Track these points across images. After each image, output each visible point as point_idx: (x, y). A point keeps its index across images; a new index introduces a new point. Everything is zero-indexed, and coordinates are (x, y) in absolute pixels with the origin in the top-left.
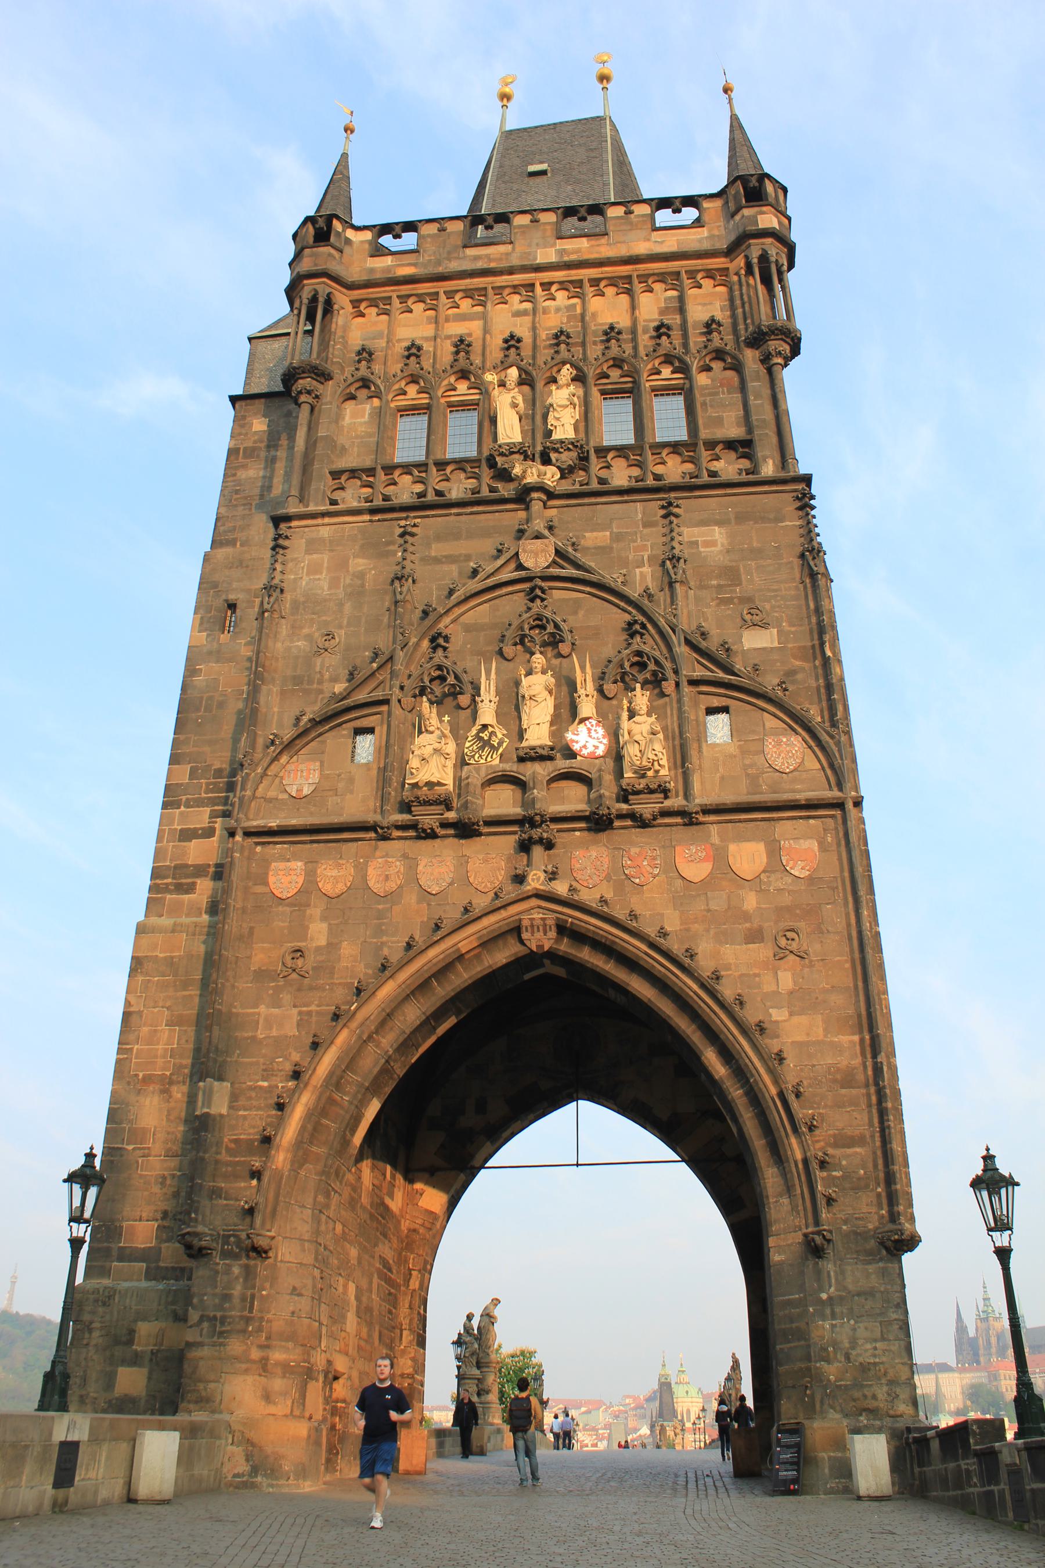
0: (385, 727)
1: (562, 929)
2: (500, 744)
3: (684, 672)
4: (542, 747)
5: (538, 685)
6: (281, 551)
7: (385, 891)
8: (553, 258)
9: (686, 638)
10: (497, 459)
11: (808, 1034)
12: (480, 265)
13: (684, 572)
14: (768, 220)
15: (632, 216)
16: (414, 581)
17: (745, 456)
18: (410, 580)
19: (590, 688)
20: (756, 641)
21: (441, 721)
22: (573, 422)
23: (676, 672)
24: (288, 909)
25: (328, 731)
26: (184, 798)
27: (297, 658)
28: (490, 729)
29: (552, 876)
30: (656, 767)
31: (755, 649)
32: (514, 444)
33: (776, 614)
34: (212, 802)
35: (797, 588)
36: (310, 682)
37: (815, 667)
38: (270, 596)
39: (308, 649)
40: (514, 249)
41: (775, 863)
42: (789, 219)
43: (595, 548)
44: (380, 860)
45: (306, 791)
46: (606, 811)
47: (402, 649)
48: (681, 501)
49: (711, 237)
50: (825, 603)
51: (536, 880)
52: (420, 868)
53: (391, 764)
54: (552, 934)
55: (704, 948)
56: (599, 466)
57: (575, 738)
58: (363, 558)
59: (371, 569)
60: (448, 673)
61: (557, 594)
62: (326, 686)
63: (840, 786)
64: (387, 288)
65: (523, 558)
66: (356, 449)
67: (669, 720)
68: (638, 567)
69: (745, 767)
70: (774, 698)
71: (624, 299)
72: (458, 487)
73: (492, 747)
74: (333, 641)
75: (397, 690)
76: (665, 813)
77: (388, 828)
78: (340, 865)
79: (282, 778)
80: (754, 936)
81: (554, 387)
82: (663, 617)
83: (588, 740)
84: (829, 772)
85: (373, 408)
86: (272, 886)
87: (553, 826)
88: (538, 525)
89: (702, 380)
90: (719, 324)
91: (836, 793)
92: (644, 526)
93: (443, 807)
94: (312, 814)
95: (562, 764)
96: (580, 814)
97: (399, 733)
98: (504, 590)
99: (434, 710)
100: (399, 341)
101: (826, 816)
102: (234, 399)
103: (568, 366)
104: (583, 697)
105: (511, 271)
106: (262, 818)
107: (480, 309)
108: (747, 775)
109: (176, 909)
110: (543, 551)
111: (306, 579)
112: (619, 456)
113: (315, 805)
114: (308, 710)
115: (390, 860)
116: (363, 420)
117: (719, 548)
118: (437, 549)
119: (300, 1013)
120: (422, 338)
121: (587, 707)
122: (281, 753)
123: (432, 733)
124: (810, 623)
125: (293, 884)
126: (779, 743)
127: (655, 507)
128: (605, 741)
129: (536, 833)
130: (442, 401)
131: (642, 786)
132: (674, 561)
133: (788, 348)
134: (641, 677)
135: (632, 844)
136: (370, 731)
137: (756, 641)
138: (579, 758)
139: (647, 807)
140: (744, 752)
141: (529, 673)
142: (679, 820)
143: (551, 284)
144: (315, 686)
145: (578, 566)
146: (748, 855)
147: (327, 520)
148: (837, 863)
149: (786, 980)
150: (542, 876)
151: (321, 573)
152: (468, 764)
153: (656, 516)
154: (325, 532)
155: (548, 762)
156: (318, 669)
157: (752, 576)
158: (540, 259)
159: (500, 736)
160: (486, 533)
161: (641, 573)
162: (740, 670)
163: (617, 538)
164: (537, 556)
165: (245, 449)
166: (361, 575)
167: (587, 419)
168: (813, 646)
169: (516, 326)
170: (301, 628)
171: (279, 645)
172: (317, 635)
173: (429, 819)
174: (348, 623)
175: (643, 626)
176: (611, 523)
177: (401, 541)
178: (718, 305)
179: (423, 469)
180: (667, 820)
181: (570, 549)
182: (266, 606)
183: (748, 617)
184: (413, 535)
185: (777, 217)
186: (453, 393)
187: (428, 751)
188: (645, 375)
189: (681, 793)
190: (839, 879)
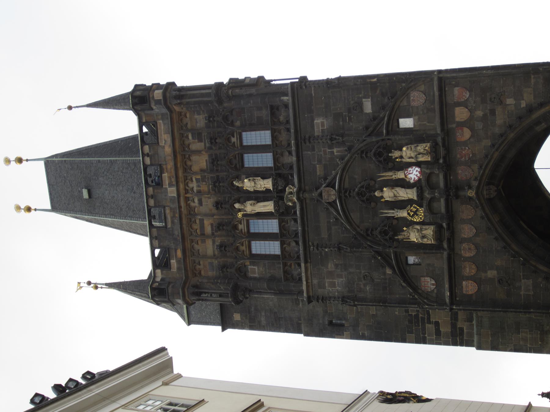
1: (488, 184)
2: (415, 208)
4: (417, 192)
5: (388, 194)
8: (174, 189)
11: (531, 94)
12: (177, 221)
14: (158, 94)
15: (150, 154)
17: (278, 109)
19: (390, 174)
20: (368, 107)
24: (482, 286)
26: (421, 335)
28: (409, 211)
29: (470, 187)
30: (427, 148)
31: (372, 108)
34: (423, 324)
38: (347, 302)
40: (168, 206)
41: (464, 104)
42: (153, 84)
44: (462, 252)
45: (433, 282)
47: (372, 247)
49: (163, 119)
51: (471, 193)
52: (466, 237)
54: (491, 187)
55: (497, 131)
64: (188, 261)
65: (330, 200)
66: (272, 271)
71: (194, 158)
76: (444, 145)
79: (428, 292)
80: (493, 112)
83: (414, 174)
85: (250, 265)
88: (315, 194)
89: (238, 123)
90: (210, 117)
92: (314, 151)
98: (345, 207)
100: (214, 255)
101: (444, 83)
102: (223, 329)
105: (180, 207)
107: (198, 221)
109: (471, 335)
110: (328, 192)
111: (337, 288)
117: (325, 121)
118: (324, 235)
119: (523, 279)
121: (400, 175)
128: (414, 167)
133: (223, 88)
134: (385, 154)
136: (407, 258)
137: (368, 107)
139: (442, 152)
141: (382, 197)
143: (185, 189)
146: (461, 114)
147: (310, 281)
149: (510, 101)
150: (470, 191)
154: (315, 282)
156: (379, 281)
158: (175, 195)
164: (331, 195)
165: (250, 322)
166: (336, 266)
169: (207, 205)
172: (364, 282)
173: (446, 234)
178: (196, 116)
180: (447, 144)
181: (327, 181)
182: (352, 304)
184: (318, 245)
185: (154, 91)
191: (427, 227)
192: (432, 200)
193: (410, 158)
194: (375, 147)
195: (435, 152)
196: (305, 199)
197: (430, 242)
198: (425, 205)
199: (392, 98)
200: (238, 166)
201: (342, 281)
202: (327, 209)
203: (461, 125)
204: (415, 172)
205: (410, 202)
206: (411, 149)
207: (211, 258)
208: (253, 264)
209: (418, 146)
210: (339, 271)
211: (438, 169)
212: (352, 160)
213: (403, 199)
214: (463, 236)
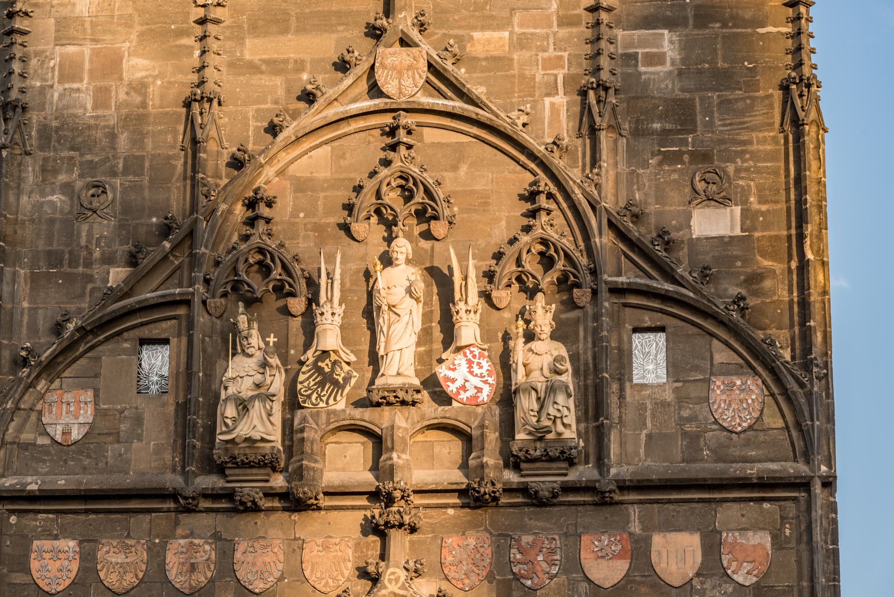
0: (184, 340)
3: (605, 277)
6: (19, 39)
7: (191, 587)
9: (609, 221)
16: (220, 104)
20: (711, 223)
23: (594, 272)
25: (101, 343)
27: (52, 221)
28: (333, 357)
33: (741, 183)
35: (775, 140)
36: (74, 263)
37: (790, 270)
39: (67, 208)
41: (712, 564)
43: (486, 59)
44: (182, 542)
45: (76, 434)
46: (489, 488)
50: (811, 174)
52: (238, 555)
53: (195, 402)
57: (451, 374)
58: (142, 56)
59: (155, 77)
60: (273, 260)
61: (430, 135)
62: (97, 271)
63: (807, 457)
65: (380, 76)
67: (581, 346)
68: (548, 95)
69: (682, 421)
70: (726, 322)
73: (335, 383)
74: (103, 198)
75: (200, 288)
76: (567, 489)
77: (193, 498)
78: (128, 547)
79: (40, 413)
82: (580, 187)
84: (794, 433)
86: (36, 575)
87: (417, 500)
91: (802, 468)
92: (560, 25)
94: (85, 469)
97: (204, 351)
104: (462, 313)
106: (15, 474)
108: (685, 434)
110: (410, 68)
113: (89, 457)
114: (72, 307)
115: (196, 541)
117: (668, 67)
118: (254, 49)
121: (468, 330)
122: (38, 377)
124: (788, 200)
125: (65, 573)
126: (731, 387)
131: (538, 453)
135: (525, 529)
136: (165, 342)
139: (545, 481)
140: (681, 399)
142: (587, 498)
144: (81, 269)
145: (461, 94)
146: (677, 553)
148: (794, 566)
150: (403, 574)
151: (81, 80)
152: (303, 408)
156: (83, 242)
157: (712, 117)
161: (552, 105)
162: (682, 277)
166: (140, 87)
168: (789, 237)
170: (56, 172)
171: (24, 199)
172: (79, 184)
174: (126, 168)
177: (199, 30)
180: (571, 498)
183: (700, 186)
187: (245, 388)
189: (592, 459)
190: (795, 589)
191: (277, 418)
193: (525, 365)
199: (742, 310)
201: (86, 109)
203: (640, 553)
204: (476, 381)
206: (558, 373)
209: (569, 396)
210: (122, 96)
214: (241, 547)
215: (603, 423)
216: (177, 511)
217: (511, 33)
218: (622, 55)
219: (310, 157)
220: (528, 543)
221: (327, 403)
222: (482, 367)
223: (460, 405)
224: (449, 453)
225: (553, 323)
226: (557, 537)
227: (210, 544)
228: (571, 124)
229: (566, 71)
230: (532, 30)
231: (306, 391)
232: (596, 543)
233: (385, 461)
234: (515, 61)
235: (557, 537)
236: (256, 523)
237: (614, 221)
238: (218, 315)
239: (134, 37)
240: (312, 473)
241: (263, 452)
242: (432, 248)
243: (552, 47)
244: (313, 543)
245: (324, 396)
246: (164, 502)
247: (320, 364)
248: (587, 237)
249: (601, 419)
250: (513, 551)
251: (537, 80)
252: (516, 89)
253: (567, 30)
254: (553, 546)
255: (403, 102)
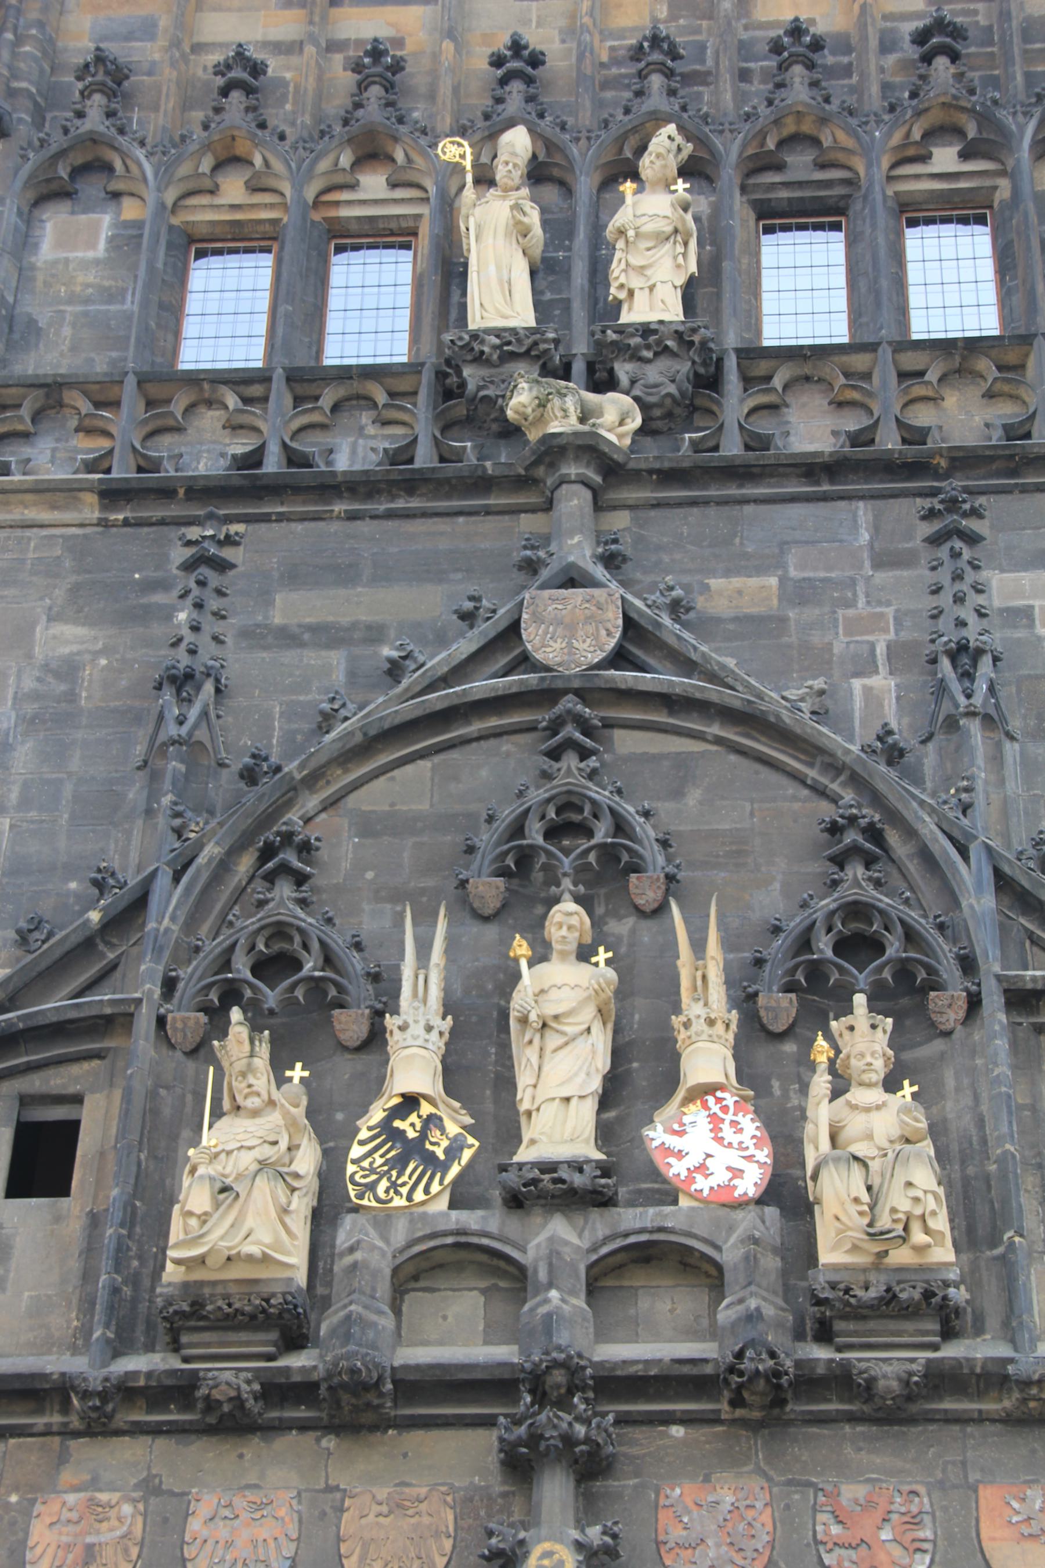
0: (118, 1094)
2: (453, 1151)
3: (997, 968)
4: (578, 1166)
5: (563, 987)
9: (998, 873)
10: (466, 372)
13: (991, 689)
18: (209, 687)
21: (281, 1081)
22: (681, 280)
28: (426, 1109)
30: (918, 1237)
32: (513, 331)
43: (736, 619)
44: (71, 1498)
47: (177, 878)
48: (982, 500)
52: (195, 1525)
56: (751, 403)
58: (76, 622)
59: (97, 654)
60: (306, 947)
61: (626, 742)
65: (532, 636)
66: (67, 331)
68: (857, 675)
72: (354, 449)
73: (430, 1159)
76: (943, 1380)
77: (104, 1396)
81: (628, 187)
82: (932, 811)
83: (710, 1150)
88: (578, 549)
93: (274, 1335)
95: (634, 1219)
96: (686, 1370)
98: (475, 727)
99: (264, 1050)
100: (198, 48)
103: (671, 128)
110: (589, 619)
112: (807, 379)
115: (103, 1497)
116: (90, 254)
118: (288, 608)
120: (265, 44)
123: (255, 1113)
127: (907, 517)
128: (764, 1155)
129: (555, 1422)
130: (316, 216)
131: (873, 1293)
132: (965, 660)
134: (863, 979)
138: (684, 1202)
139: (890, 1361)
141: (541, 954)
145: (688, 665)
153: (909, 536)
155: (595, 1214)
159: (453, 1129)
160: (428, 570)
161: (867, 690)
163: (800, 593)
164: (571, 634)
166: (68, 670)
167: (717, 283)
173: (230, 1371)
175: (874, 834)
176: (782, 552)
179: (256, 390)
181: (666, 620)
184: (223, 566)
186: (345, 196)
188: (885, 164)
192: (507, 1275)
194: (913, 915)
195: (889, 1306)
196: (548, 506)
197: (176, 1231)
198: (470, 1219)
200: (776, 178)
202: (468, 617)
205: (501, 1124)
207: (182, 24)
208: (128, 239)
211: (753, 1318)
212: (812, 774)
213: (524, 1079)
215: (1011, 1243)
216: (67, 1433)
217: (783, 580)
218: (1002, 611)
219: (393, 779)
220: (856, 1502)
221: (409, 1198)
222: (741, 1131)
223: (695, 1204)
224: (672, 1311)
225: (891, 1053)
226: (921, 1489)
227: (134, 1501)
228: (906, 721)
229: (892, 636)
230: (822, 574)
231: (364, 1177)
232: (1015, 1505)
233: (532, 1310)
234: (792, 623)
235: (921, 1489)
236: (241, 1456)
237: (1006, 869)
238: (189, 1047)
239: (60, 594)
240: (371, 1334)
241: (266, 1290)
242: (633, 931)
243: (861, 602)
244: (368, 1497)
245: (404, 1184)
246: (40, 1411)
247: (397, 1124)
248: (955, 902)
249: (1011, 1233)
250: (821, 1517)
251: (836, 651)
252: (796, 667)
253: (890, 574)
254: (914, 1509)
255: (575, 676)
